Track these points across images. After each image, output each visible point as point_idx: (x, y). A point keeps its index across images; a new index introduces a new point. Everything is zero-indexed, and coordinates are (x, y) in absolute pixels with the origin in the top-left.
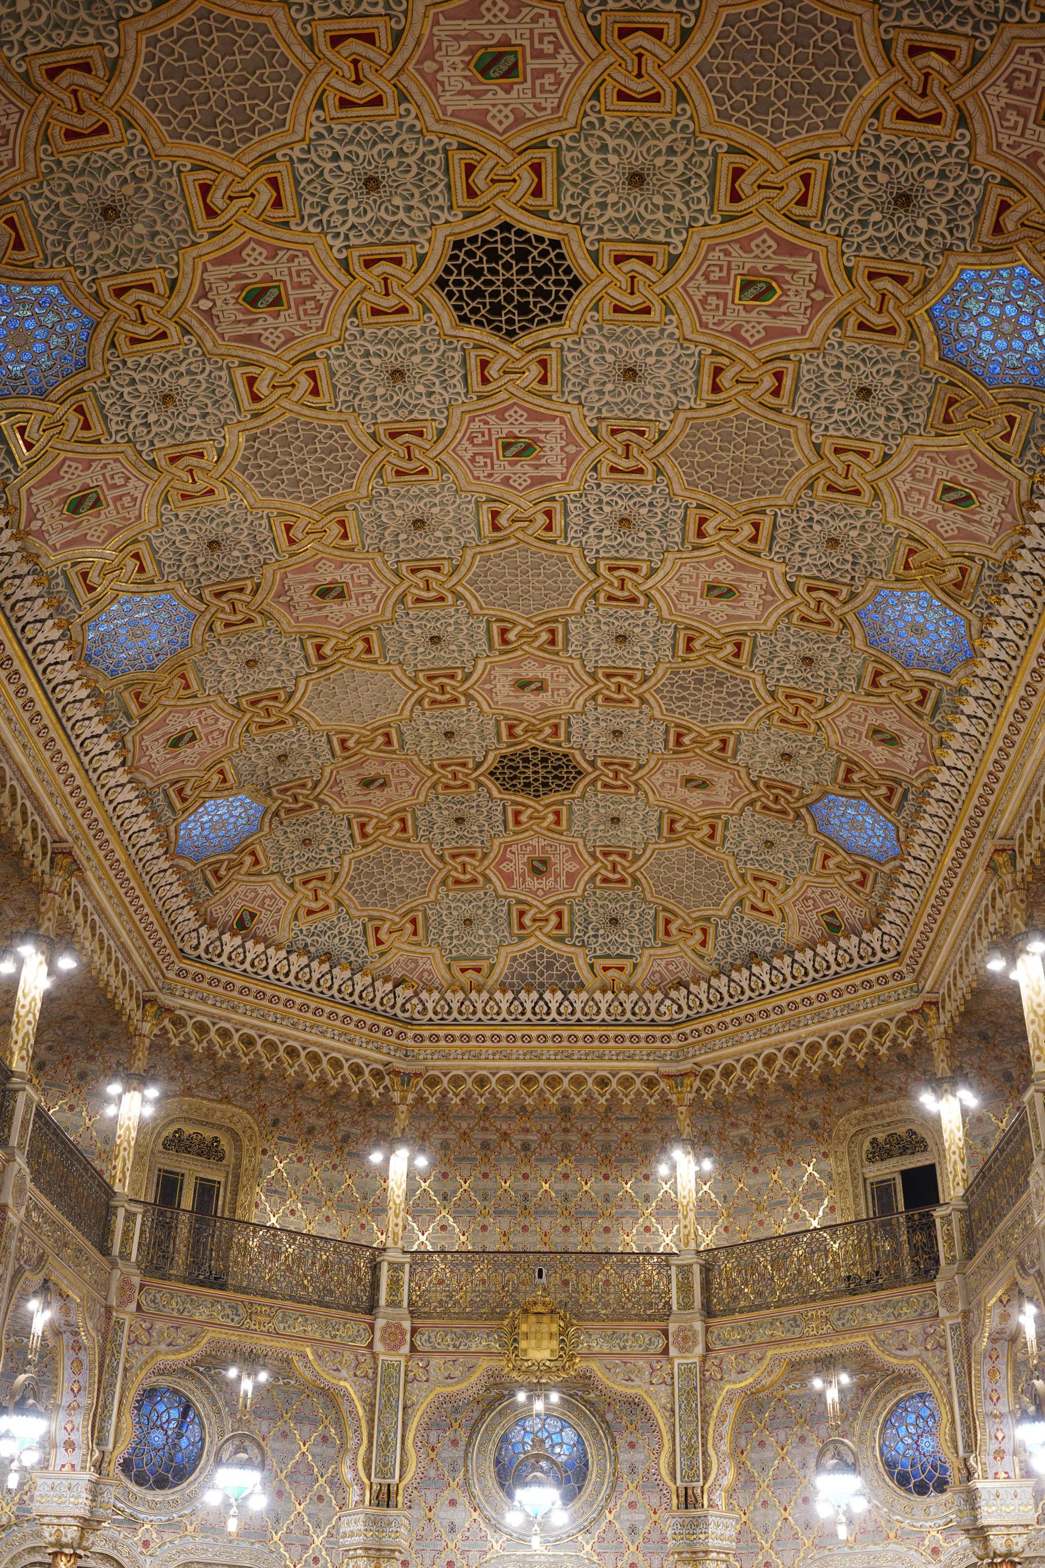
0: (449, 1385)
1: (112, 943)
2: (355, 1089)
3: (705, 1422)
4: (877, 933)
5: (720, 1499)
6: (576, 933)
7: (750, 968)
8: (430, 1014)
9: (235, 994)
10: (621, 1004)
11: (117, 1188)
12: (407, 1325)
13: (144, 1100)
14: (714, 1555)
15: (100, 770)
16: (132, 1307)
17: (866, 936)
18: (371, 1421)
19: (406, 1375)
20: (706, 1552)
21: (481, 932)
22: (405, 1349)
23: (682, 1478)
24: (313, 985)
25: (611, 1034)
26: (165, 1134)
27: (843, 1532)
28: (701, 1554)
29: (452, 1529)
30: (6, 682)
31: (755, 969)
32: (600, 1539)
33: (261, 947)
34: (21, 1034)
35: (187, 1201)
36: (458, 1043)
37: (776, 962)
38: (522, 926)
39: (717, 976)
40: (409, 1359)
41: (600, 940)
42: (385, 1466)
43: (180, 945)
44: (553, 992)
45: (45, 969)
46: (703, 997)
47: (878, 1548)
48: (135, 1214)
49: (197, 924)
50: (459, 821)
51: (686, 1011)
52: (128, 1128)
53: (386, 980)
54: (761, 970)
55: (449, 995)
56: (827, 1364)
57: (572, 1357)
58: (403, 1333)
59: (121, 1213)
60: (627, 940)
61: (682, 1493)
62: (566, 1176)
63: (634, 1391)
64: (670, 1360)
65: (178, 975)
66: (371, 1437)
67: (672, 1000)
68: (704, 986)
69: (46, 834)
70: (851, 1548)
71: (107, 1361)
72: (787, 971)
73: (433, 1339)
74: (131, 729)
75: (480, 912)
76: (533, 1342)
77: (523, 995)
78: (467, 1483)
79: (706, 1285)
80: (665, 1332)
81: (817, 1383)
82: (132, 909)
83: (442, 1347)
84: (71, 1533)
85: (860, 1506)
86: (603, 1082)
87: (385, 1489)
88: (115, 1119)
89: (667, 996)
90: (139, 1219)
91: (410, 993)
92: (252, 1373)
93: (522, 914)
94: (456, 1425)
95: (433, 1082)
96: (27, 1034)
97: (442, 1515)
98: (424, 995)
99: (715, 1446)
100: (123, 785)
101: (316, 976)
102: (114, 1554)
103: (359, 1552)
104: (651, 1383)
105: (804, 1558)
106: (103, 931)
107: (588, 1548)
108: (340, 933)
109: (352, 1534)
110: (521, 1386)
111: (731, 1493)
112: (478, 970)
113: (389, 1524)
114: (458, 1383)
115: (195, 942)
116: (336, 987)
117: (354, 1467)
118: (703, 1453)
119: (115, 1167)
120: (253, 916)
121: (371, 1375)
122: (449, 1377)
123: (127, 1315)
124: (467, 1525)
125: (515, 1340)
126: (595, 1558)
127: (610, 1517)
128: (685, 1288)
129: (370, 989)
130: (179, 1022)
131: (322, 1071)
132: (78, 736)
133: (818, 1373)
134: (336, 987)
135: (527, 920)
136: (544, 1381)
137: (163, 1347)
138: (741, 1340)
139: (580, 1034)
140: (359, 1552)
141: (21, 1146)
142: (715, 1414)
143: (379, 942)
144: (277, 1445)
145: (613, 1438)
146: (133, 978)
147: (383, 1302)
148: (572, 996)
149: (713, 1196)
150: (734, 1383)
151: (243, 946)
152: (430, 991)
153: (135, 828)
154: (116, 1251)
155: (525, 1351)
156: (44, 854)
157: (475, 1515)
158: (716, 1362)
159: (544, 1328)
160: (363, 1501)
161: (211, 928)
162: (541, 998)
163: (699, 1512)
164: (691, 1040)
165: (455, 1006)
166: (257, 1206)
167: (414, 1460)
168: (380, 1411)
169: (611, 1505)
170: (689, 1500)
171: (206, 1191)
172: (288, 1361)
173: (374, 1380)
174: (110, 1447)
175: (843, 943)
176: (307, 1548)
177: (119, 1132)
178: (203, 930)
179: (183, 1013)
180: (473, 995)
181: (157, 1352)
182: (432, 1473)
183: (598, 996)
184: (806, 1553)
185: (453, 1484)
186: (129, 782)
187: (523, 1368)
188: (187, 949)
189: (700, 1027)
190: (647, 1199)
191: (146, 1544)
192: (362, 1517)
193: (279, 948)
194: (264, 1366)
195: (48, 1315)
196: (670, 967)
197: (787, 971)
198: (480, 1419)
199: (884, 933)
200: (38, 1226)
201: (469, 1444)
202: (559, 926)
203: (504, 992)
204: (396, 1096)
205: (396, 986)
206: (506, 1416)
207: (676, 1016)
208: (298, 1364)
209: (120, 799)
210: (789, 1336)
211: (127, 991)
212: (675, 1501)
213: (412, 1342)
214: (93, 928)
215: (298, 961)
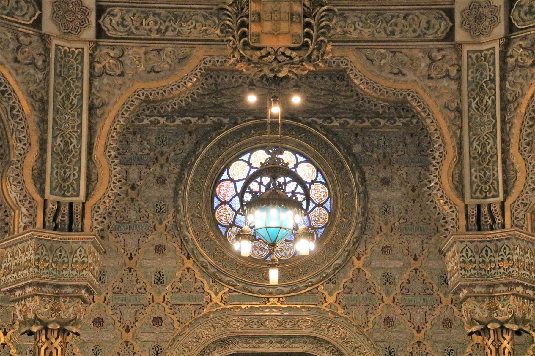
14: (520, 289)
19: (92, 67)
22: (90, 33)
28: (502, 288)
29: (160, 280)
32: (348, 290)
40: (96, 47)
42: (64, 180)
57: (320, 45)
58: (85, 12)
61: (472, 211)
63: (405, 87)
64: (458, 48)
66: (43, 143)
73: (128, 22)
76: (268, 26)
83: (142, 33)
87: (65, 210)
94: (162, 160)
97: (145, 263)
103: (29, 290)
104: (430, 77)
107: (331, 300)
110: (252, 86)
113: (73, 252)
114: (163, 78)
118: (504, 162)
121: (40, 63)
122: (152, 70)
124: (178, 274)
125: (244, 24)
126: (341, 311)
127: (359, 264)
136: (281, 75)
140: (29, 290)
142: (522, 109)
145: (362, 173)
157: (189, 263)
160: (33, 223)
163: (498, 233)
167: (107, 173)
168: (56, 111)
169: (360, 250)
185: (160, 228)
187: (255, 59)
192: (32, 243)
198: (193, 152)
201: (179, 180)
206: (225, 146)
212: (462, 222)
213: (98, 26)
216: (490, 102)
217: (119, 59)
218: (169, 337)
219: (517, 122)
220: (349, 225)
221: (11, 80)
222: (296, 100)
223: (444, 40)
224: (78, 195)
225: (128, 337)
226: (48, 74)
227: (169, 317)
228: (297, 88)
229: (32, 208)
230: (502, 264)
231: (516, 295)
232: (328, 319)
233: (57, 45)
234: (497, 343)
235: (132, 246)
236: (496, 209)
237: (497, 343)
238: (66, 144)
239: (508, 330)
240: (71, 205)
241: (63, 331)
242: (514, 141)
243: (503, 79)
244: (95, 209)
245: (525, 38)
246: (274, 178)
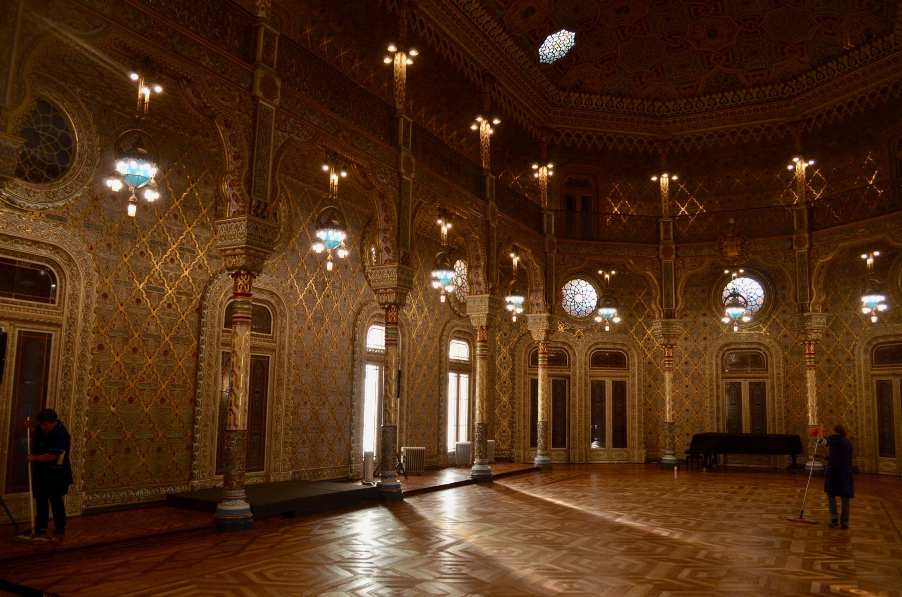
0: (694, 269)
1: (520, 107)
2: (641, 150)
3: (810, 276)
4: (892, 36)
5: (819, 308)
6: (737, 62)
7: (826, 65)
8: (672, 112)
9: (580, 118)
10: (763, 92)
11: (543, 206)
12: (673, 247)
13: (548, 170)
15: (495, 36)
16: (555, 251)
17: (886, 39)
18: (661, 286)
20: (812, 330)
21: (690, 70)
22: (674, 257)
23: (800, 301)
24: (614, 108)
25: (759, 107)
26: (565, 180)
27: (874, 319)
30: (442, 10)
31: (829, 65)
32: (770, 326)
33: (588, 96)
34: (484, 153)
35: (578, 206)
36: (686, 123)
37: (840, 59)
38: (709, 63)
39: (810, 70)
41: (749, 63)
43: (552, 102)
44: (729, 92)
45: (488, 126)
46: (804, 82)
47: (899, 325)
48: (551, 215)
49: (558, 91)
50: (668, 19)
51: (797, 91)
52: (543, 181)
53: (648, 100)
54: (833, 65)
55: (679, 102)
56: (868, 249)
57: (748, 254)
58: (672, 250)
59: (545, 216)
60: (763, 61)
62: (747, 175)
64: (794, 251)
65: (554, 114)
67: (789, 86)
68: (804, 77)
69: (478, 69)
70: (886, 325)
71: (548, 273)
72: (846, 63)
74: (504, 15)
75: (687, 60)
76: (729, 249)
77: (714, 96)
78: (709, 308)
79: (811, 218)
80: (791, 240)
81: (864, 256)
82: (525, 91)
84: (543, 336)
85: (882, 308)
86: (757, 131)
87: (669, 312)
88: (538, 178)
89: (786, 85)
90: (553, 217)
91: (660, 104)
92: (608, 272)
93: (708, 57)
95: (676, 142)
96: (486, 153)
97: (700, 319)
98: (667, 104)
99: (814, 286)
100: (506, 40)
101: (615, 104)
102: (567, 341)
104: (785, 262)
105: (864, 331)
106: (515, 103)
108: (623, 82)
109: (657, 329)
110: (726, 268)
111: (824, 304)
112: (691, 87)
113: (672, 324)
114: (696, 269)
115: (558, 99)
116: (625, 107)
117: (655, 304)
119: (540, 198)
120: (582, 82)
122: (694, 266)
123: (553, 255)
124: (711, 323)
126: (768, 334)
127: (774, 317)
128: (800, 220)
129: (641, 105)
130: (558, 135)
131: (625, 145)
132: (480, 24)
133: (864, 253)
134: (625, 107)
135: (711, 60)
137: (570, 265)
139: (744, 110)
141: (491, 198)
142: (815, 272)
143: (642, 83)
144: (628, 297)
146: (534, 119)
147: (662, 238)
148: (738, 92)
149: (820, 175)
150: (823, 259)
151: (579, 97)
152: (670, 101)
153: (517, 57)
154: (545, 231)
155: (726, 253)
156: (479, 77)
157: (714, 319)
158: (815, 251)
159: (735, 243)
160: (660, 317)
161: (564, 91)
162: (723, 96)
164: (800, 104)
165: (683, 106)
166: (608, 204)
170: (803, 309)
171: (585, 201)
172: (624, 266)
173: (661, 270)
174: (554, 303)
175: (874, 44)
176: (645, 335)
177: (540, 183)
178: (561, 93)
179: (559, 130)
180: (690, 100)
181: (568, 267)
182: (695, 304)
183: (751, 90)
184: (865, 328)
186: (509, 37)
188: (556, 103)
189: (804, 97)
190: (788, 181)
191: (579, 337)
192: (660, 323)
193: (596, 95)
195: (518, 258)
196: (787, 70)
197: (846, 63)
199: (896, 35)
200: (505, 226)
202: (728, 60)
203: (705, 96)
204: (660, 151)
205: (653, 101)
207: (792, 94)
208: (628, 266)
209: (507, 46)
210: (849, 236)
211: (532, 125)
214: (510, 103)
215: (606, 99)
217: (683, 264)
218: (709, 343)
219: (813, 277)
220: (770, 304)
221: (651, 275)
222: (741, 271)
224: (672, 307)
225: (695, 344)
226: (661, 272)
227: (709, 337)
228: (741, 267)
229: (660, 311)
231: (814, 333)
232: (763, 336)
234: (809, 347)
235: (695, 314)
236: (807, 305)
238: (668, 292)
241: (672, 347)
242: (813, 283)
243: (809, 262)
244: (678, 311)
246: (735, 297)
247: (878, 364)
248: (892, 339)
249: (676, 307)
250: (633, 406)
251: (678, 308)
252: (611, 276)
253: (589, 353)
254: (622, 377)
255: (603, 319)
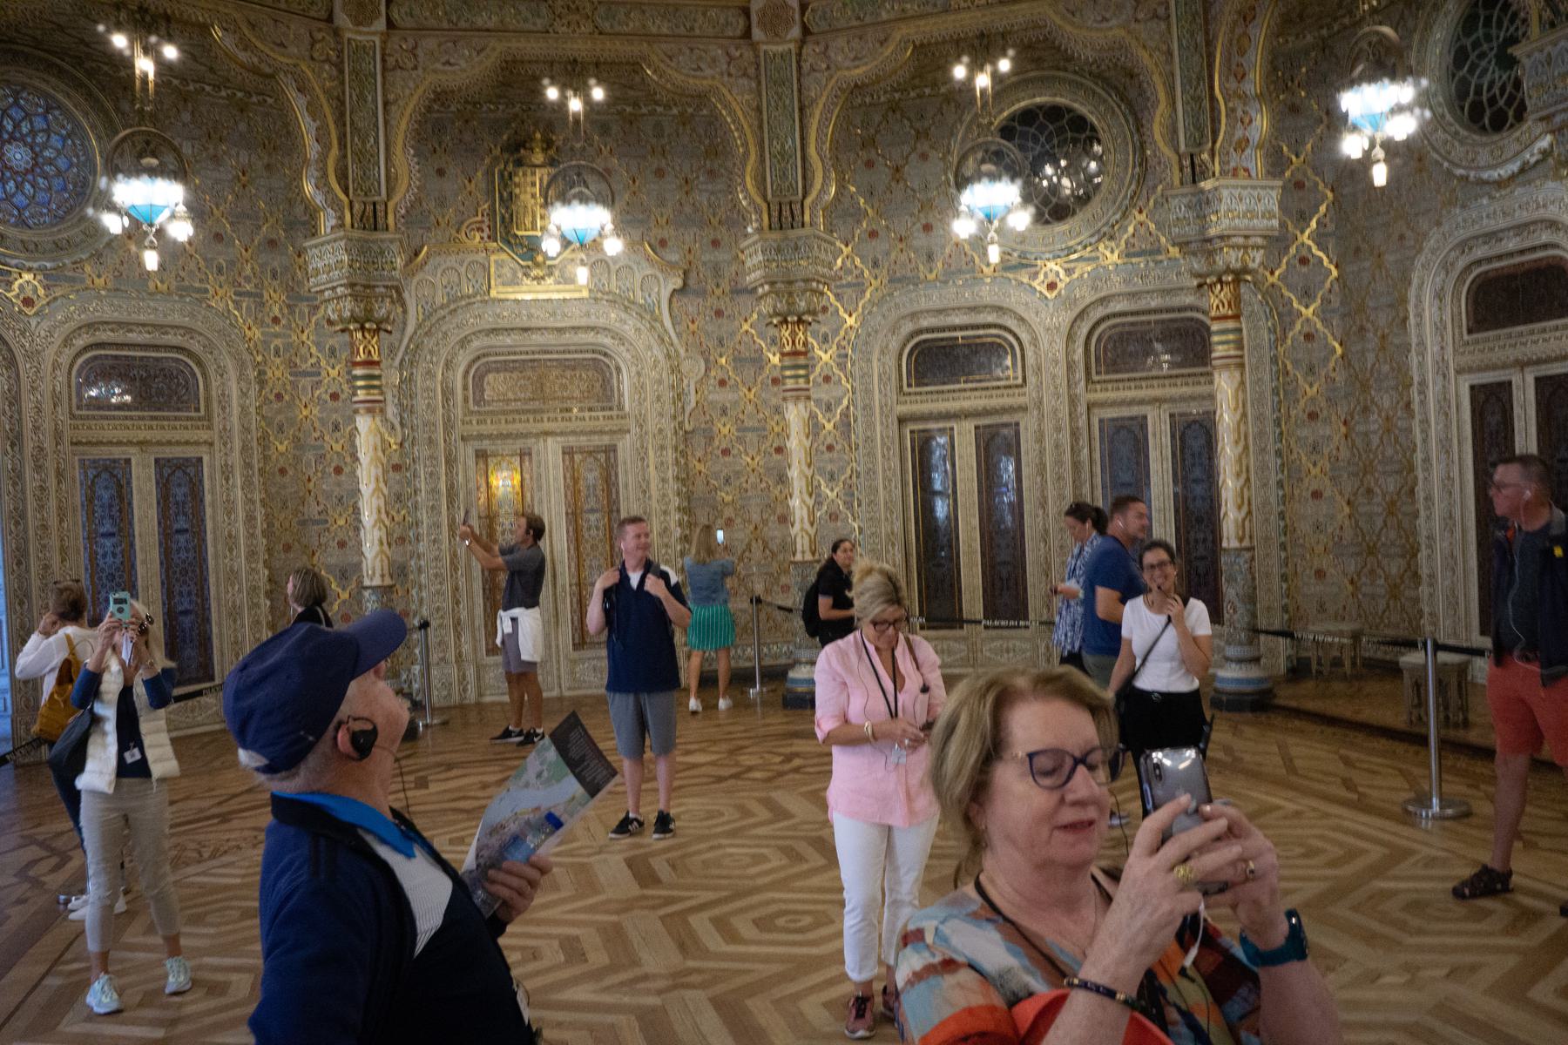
19: (384, 61)
22: (380, 25)
64: (754, 46)
121: (334, 58)
138: (858, 18)
160: (342, 225)
163: (799, 232)
194: (170, 39)
216: (787, 102)
217: (413, 52)
223: (741, 38)
230: (802, 262)
233: (349, 40)
237: (793, 334)
239: (804, 322)
240: (374, 204)
245: (818, 43)
247: (917, 385)
248: (957, 320)
249: (389, 196)
250: (231, 541)
251: (396, 198)
252: (160, 63)
253: (65, 360)
254: (187, 443)
255: (135, 223)
